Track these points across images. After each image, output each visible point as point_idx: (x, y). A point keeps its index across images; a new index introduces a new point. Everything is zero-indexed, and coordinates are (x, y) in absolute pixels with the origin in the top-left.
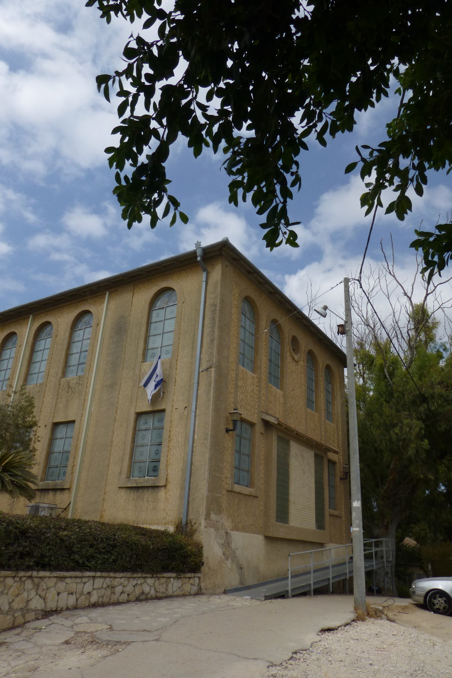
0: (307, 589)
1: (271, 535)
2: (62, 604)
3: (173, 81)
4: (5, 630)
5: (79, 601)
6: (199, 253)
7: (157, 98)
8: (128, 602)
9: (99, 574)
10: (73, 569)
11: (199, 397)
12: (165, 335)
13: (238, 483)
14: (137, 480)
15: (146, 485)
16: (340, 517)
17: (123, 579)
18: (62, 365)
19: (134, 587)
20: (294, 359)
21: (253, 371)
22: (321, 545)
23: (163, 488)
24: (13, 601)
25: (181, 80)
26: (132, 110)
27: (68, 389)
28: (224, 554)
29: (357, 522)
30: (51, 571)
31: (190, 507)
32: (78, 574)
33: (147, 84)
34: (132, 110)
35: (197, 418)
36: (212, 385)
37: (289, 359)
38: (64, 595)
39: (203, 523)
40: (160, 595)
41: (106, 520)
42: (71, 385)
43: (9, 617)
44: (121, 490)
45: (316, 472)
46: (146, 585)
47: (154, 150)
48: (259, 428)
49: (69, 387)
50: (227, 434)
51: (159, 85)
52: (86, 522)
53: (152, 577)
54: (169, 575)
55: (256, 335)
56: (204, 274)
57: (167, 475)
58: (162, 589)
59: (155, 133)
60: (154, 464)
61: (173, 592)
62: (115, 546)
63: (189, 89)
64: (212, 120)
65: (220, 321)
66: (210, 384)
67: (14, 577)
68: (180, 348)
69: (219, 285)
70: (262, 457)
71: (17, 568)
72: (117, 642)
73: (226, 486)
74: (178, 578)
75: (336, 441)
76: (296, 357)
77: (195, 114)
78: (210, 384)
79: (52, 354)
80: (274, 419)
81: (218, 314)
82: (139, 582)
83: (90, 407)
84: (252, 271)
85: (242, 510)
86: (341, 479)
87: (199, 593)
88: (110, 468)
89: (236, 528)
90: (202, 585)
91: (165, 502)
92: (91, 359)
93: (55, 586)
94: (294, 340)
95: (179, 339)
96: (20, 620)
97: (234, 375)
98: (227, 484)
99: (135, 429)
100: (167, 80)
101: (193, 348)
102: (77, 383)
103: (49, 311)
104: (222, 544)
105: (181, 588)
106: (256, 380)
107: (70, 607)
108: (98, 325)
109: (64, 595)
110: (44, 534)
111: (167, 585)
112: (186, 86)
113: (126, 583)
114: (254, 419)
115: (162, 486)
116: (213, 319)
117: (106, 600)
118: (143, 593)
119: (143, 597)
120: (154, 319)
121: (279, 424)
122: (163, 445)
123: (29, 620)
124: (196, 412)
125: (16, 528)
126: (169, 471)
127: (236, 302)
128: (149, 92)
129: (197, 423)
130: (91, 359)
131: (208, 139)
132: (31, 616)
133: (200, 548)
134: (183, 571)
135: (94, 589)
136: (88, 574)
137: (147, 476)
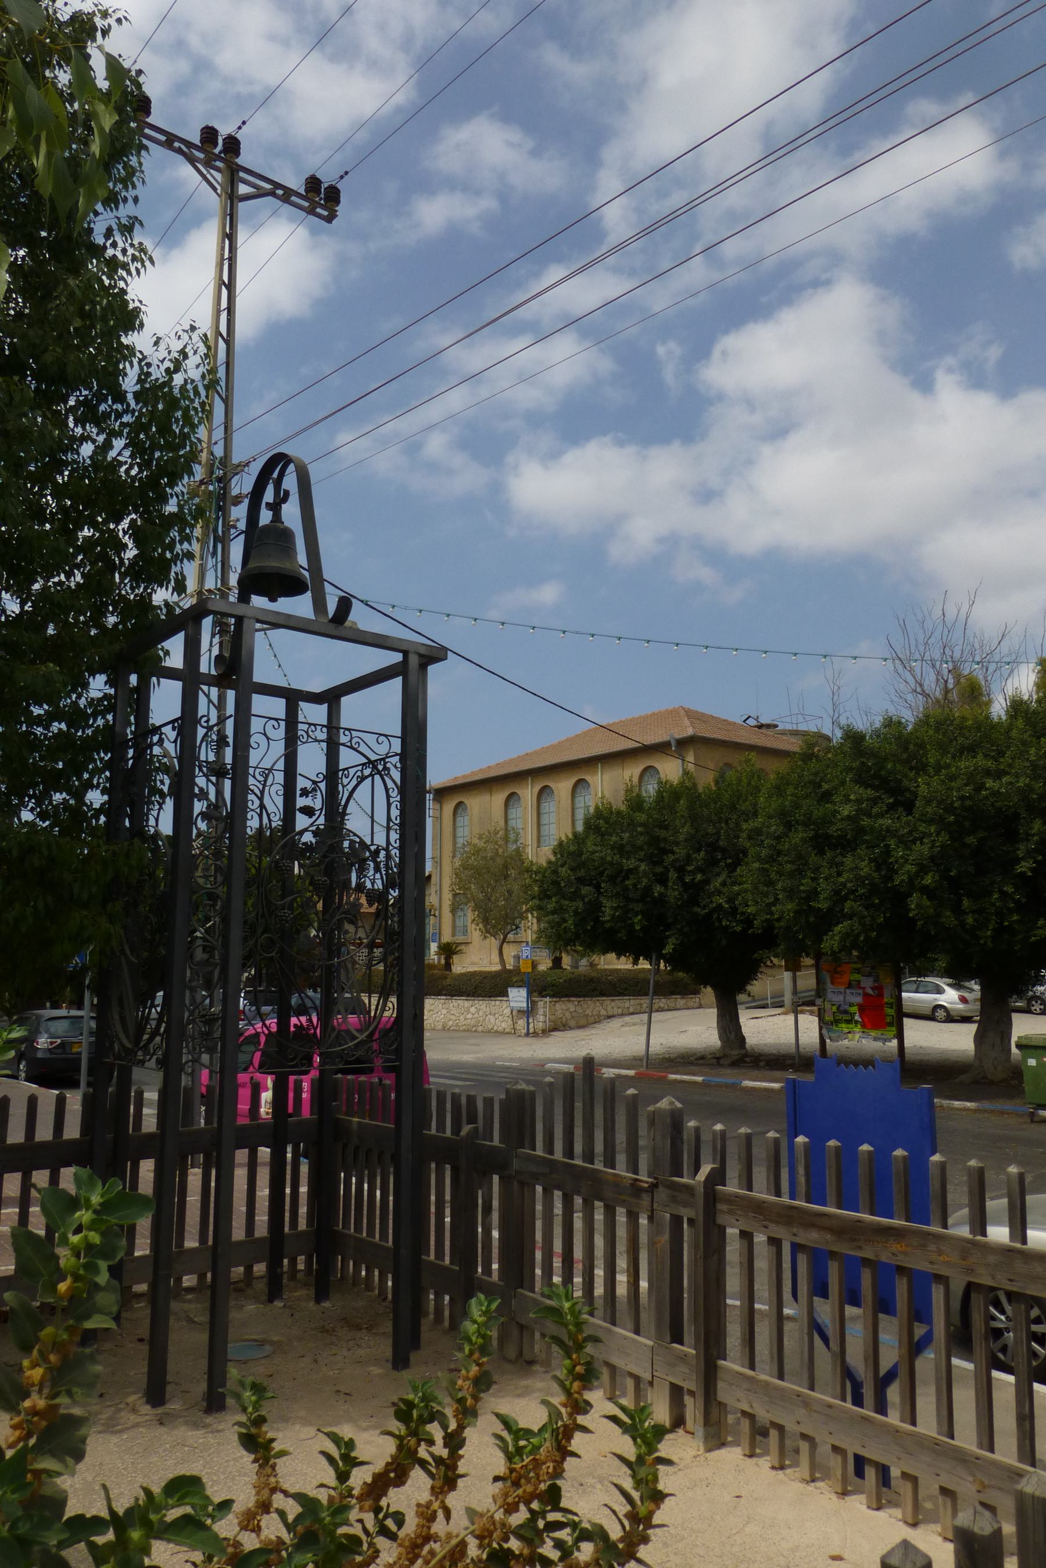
71: (592, 996)
87: (700, 1007)
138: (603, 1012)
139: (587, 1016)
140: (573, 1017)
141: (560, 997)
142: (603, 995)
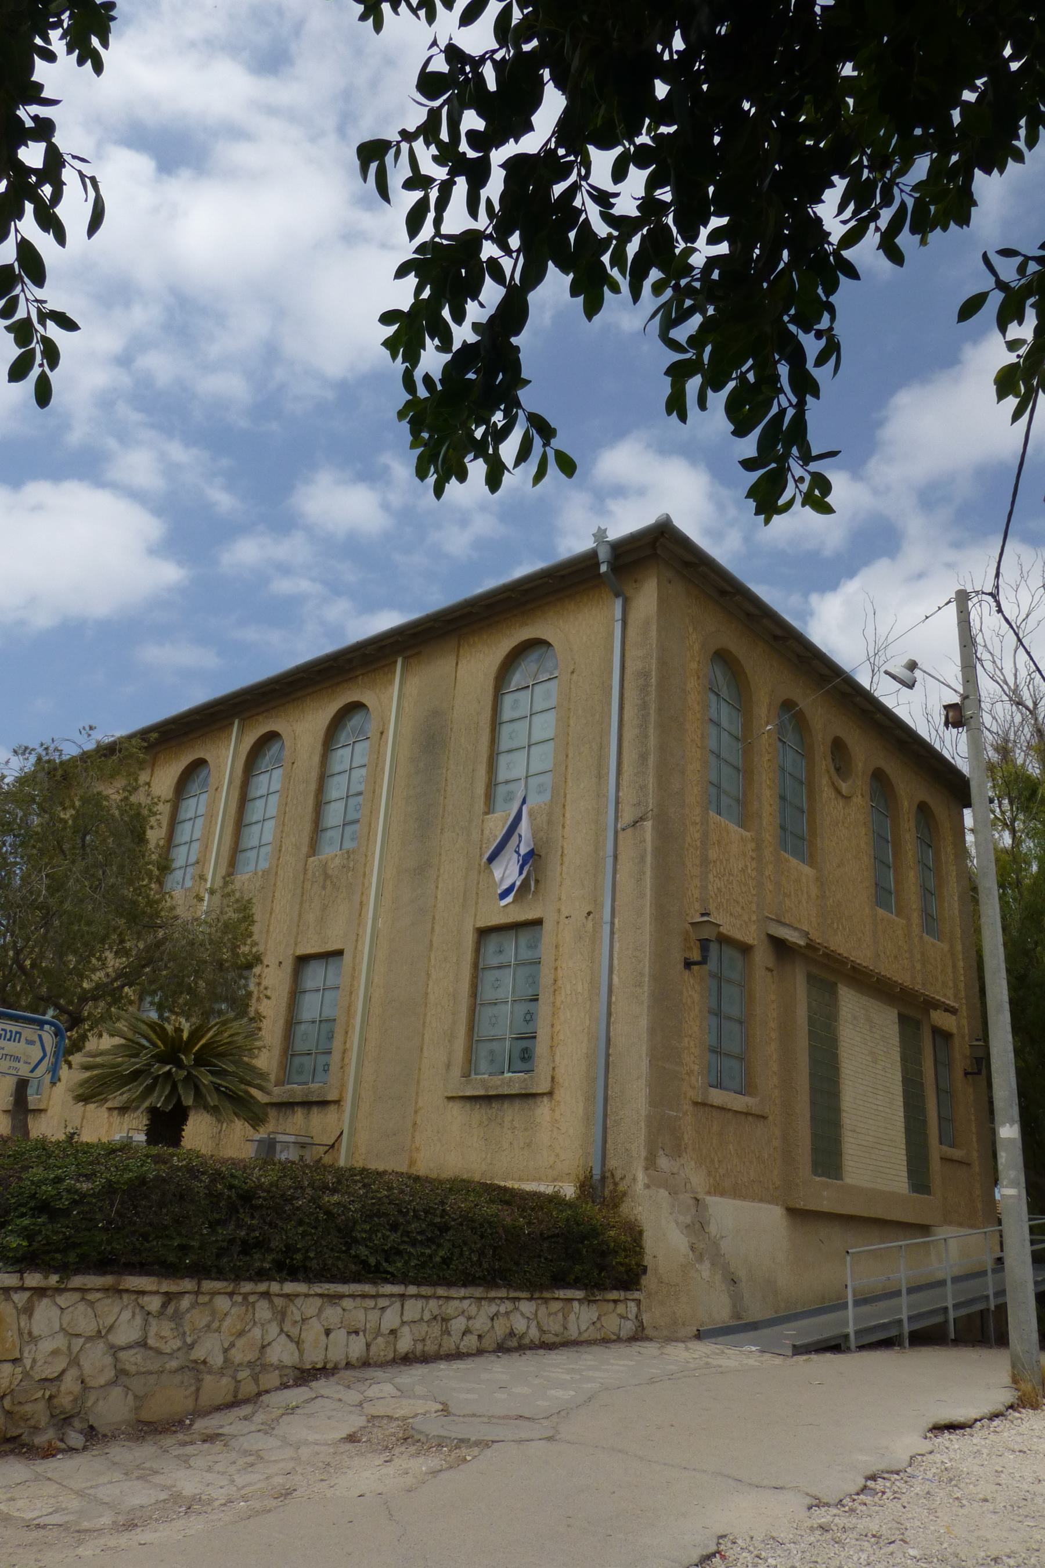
0: (893, 1332)
1: (801, 1205)
2: (336, 1355)
3: (531, 144)
4: (218, 1409)
5: (373, 1349)
6: (603, 554)
7: (494, 188)
8: (480, 1352)
9: (412, 1290)
10: (357, 1279)
11: (618, 888)
12: (533, 749)
13: (719, 1085)
14: (486, 1082)
15: (506, 1091)
16: (969, 1165)
17: (467, 1302)
18: (307, 826)
19: (492, 1319)
20: (838, 791)
21: (743, 824)
22: (924, 1229)
23: (545, 1099)
24: (232, 1345)
25: (549, 140)
26: (438, 222)
27: (325, 881)
28: (692, 1249)
29: (1012, 1174)
30: (308, 1280)
31: (609, 1141)
32: (368, 1288)
33: (472, 154)
34: (438, 222)
35: (616, 936)
36: (649, 859)
37: (827, 792)
38: (339, 1336)
39: (641, 1177)
40: (549, 1338)
41: (422, 1169)
42: (330, 872)
43: (225, 1381)
44: (451, 1104)
45: (904, 1059)
46: (518, 1315)
47: (491, 310)
48: (763, 956)
49: (327, 876)
50: (687, 972)
51: (499, 156)
52: (380, 1174)
53: (531, 1299)
54: (569, 1293)
55: (745, 739)
56: (618, 604)
57: (554, 1069)
58: (554, 1325)
59: (495, 269)
60: (524, 1044)
61: (580, 1333)
62: (444, 1228)
63: (572, 158)
64: (624, 226)
65: (660, 710)
66: (642, 859)
67: (231, 1295)
68: (569, 777)
69: (654, 627)
70: (772, 1025)
71: (238, 1276)
72: (462, 1441)
73: (691, 1093)
74: (589, 1301)
75: (951, 984)
76: (844, 787)
77: (583, 216)
78: (642, 859)
79: (286, 804)
80: (796, 934)
81: (653, 695)
82: (502, 1309)
83: (375, 919)
84: (729, 589)
85: (731, 1146)
86: (966, 1074)
87: (639, 1336)
88: (426, 1053)
89: (718, 1190)
90: (646, 1318)
91: (552, 1131)
92: (371, 812)
93: (318, 1315)
94: (838, 747)
95: (567, 756)
96: (249, 1388)
97: (697, 836)
98: (694, 1088)
99: (476, 965)
100: (516, 142)
101: (601, 777)
102: (344, 867)
103: (273, 708)
104: (687, 1226)
105: (598, 1325)
106: (751, 845)
107: (354, 1361)
108: (382, 733)
109: (339, 1336)
110: (290, 1200)
111: (565, 1318)
112: (561, 152)
113: (473, 1310)
114: (750, 935)
115: (542, 1095)
116: (644, 706)
117: (431, 1348)
118: (512, 1334)
119: (513, 1343)
120: (507, 714)
121: (811, 946)
122: (540, 1001)
123: (268, 1387)
124: (612, 924)
125: (231, 1187)
126: (557, 1059)
127: (694, 665)
128: (478, 174)
129: (617, 946)
130: (371, 812)
131: (615, 273)
132: (271, 1379)
133: (636, 1234)
134: (601, 1287)
135: (403, 1323)
136: (389, 1289)
137: (509, 1071)
138: (282, 1353)
139: (197, 1368)
140: (121, 1373)
141: (65, 1270)
142: (293, 1273)
